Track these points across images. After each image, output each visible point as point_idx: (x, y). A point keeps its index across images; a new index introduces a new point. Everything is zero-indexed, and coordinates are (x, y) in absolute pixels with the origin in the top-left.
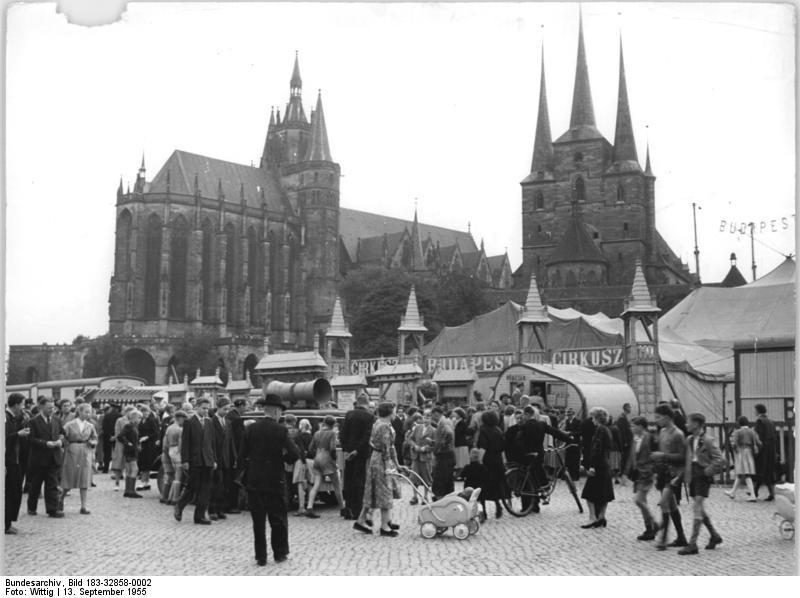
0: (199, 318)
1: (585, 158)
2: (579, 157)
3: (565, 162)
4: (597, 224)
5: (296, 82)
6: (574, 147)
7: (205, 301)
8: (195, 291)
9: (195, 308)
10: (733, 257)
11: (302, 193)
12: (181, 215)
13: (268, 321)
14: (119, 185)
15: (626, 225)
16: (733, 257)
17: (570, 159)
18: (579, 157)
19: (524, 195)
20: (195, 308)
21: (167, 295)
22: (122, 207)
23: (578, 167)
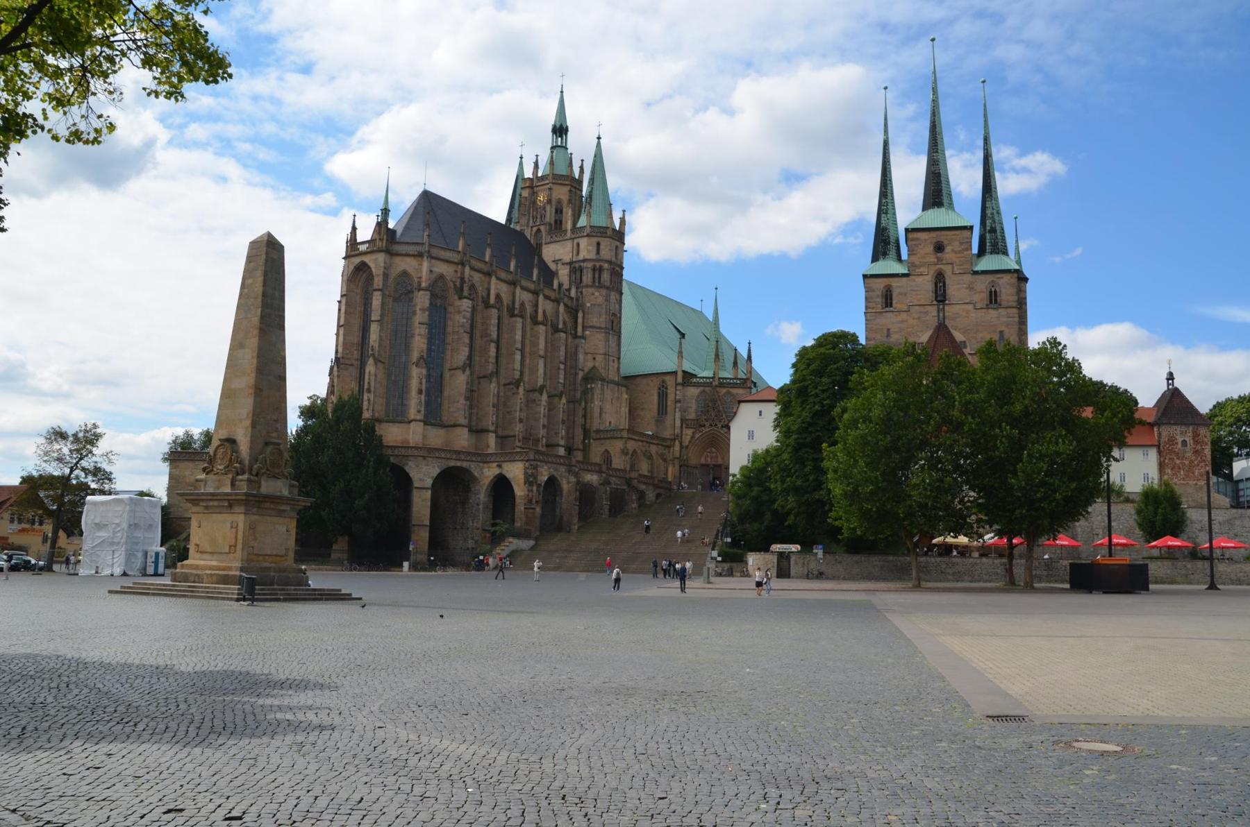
0: (463, 421)
1: (948, 249)
2: (939, 248)
4: (965, 332)
5: (560, 130)
6: (934, 234)
7: (472, 396)
8: (458, 383)
9: (456, 408)
10: (1171, 377)
11: (576, 269)
12: (441, 277)
13: (542, 432)
14: (350, 230)
15: (1001, 332)
16: (1171, 377)
17: (930, 249)
18: (939, 248)
19: (868, 290)
20: (456, 408)
21: (424, 388)
22: (357, 260)
23: (939, 260)
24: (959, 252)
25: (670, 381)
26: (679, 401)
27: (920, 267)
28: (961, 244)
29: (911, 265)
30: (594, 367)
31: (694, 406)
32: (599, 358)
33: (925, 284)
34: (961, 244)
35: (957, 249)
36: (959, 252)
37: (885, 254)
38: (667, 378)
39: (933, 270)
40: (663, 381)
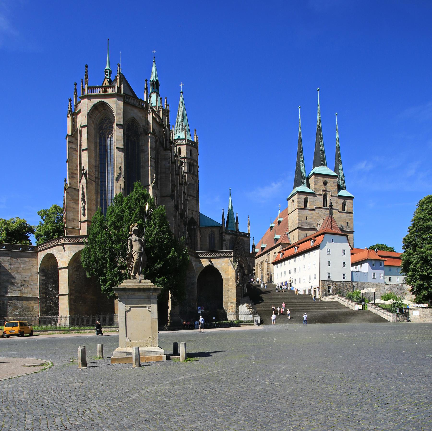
2: (325, 183)
3: (320, 184)
18: (325, 183)
23: (326, 188)
24: (333, 186)
25: (216, 231)
26: (225, 240)
27: (318, 191)
28: (334, 183)
29: (315, 189)
30: (192, 218)
31: (228, 245)
32: (195, 213)
33: (321, 198)
34: (334, 183)
35: (332, 185)
36: (333, 186)
37: (303, 183)
38: (215, 230)
39: (324, 193)
40: (212, 231)
